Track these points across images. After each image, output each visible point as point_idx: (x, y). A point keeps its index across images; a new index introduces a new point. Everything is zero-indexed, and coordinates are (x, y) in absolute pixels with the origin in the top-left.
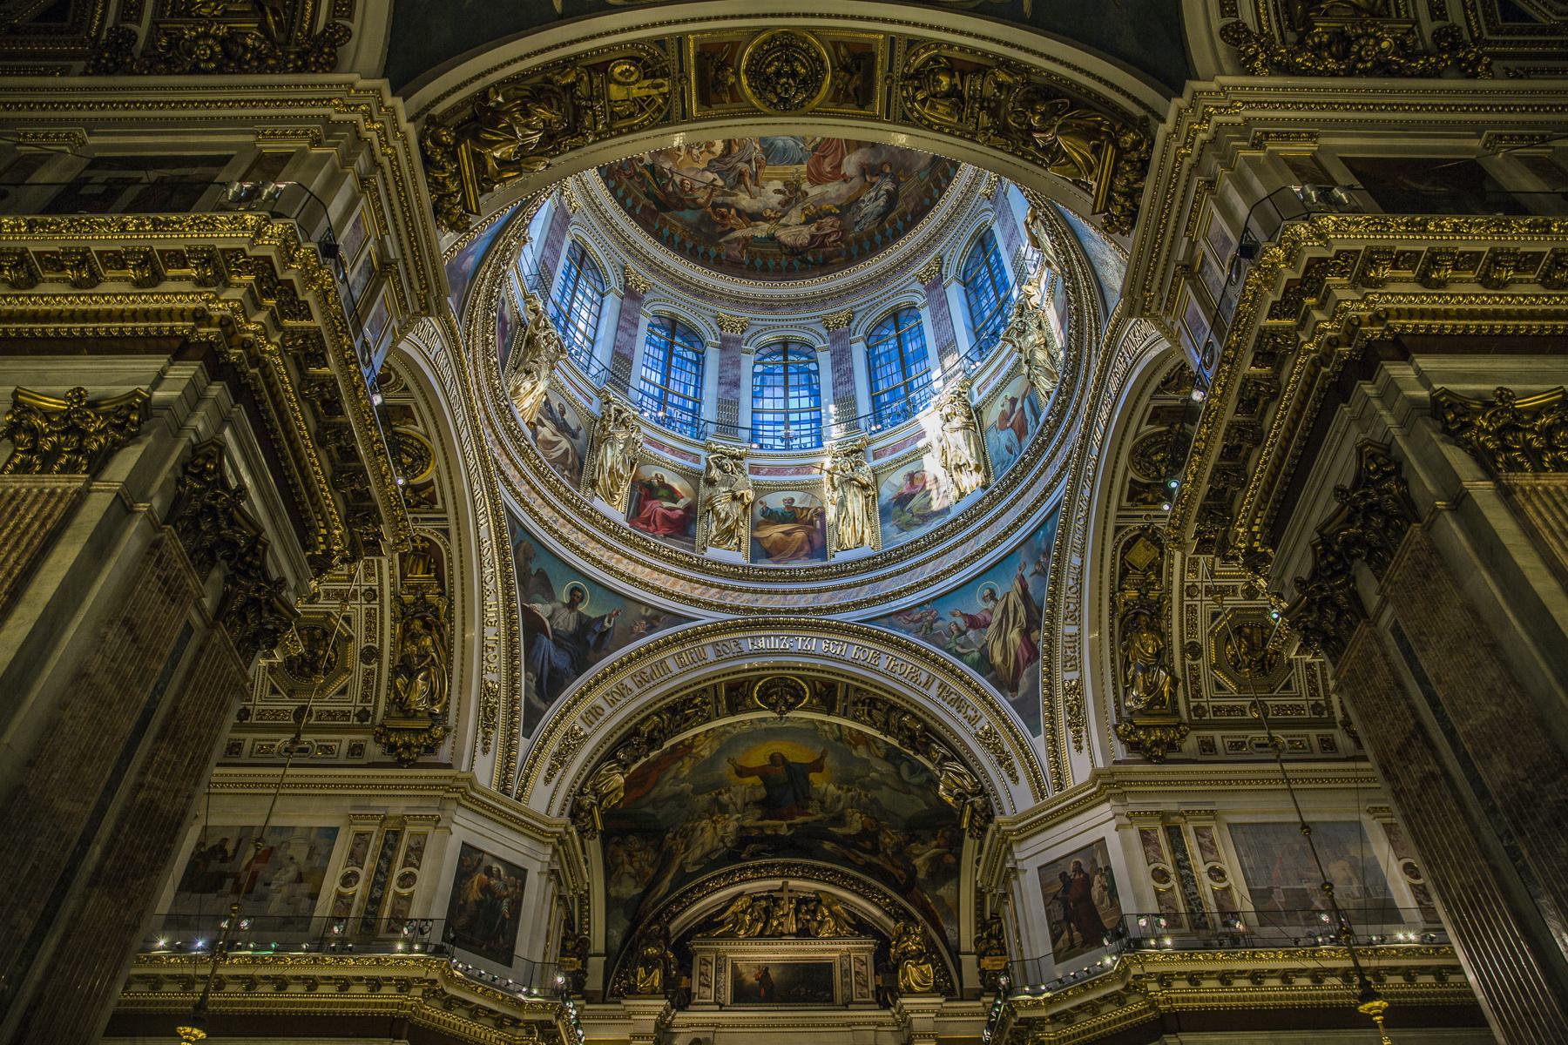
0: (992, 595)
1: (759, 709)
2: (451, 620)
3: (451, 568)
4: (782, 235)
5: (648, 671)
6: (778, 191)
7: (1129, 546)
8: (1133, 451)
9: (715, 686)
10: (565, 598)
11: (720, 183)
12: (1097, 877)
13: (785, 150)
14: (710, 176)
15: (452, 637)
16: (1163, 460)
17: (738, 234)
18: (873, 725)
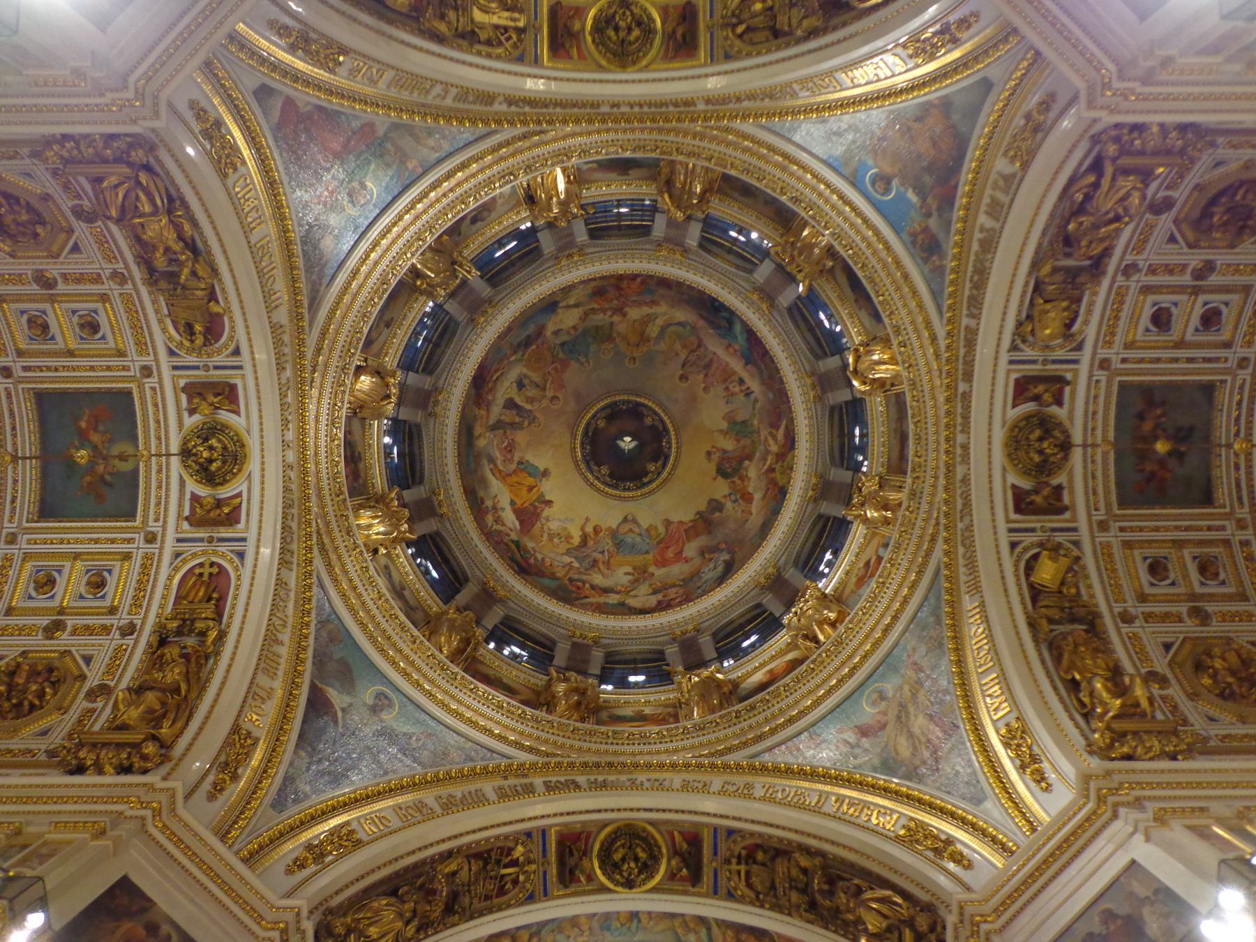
0: (882, 697)
1: (603, 889)
2: (217, 654)
3: (235, 597)
4: (632, 602)
5: (459, 795)
6: (628, 574)
8: (1006, 445)
9: (544, 832)
10: (370, 701)
11: (576, 565)
12: (1146, 912)
13: (633, 546)
14: (567, 559)
15: (212, 672)
16: (1041, 439)
17: (591, 600)
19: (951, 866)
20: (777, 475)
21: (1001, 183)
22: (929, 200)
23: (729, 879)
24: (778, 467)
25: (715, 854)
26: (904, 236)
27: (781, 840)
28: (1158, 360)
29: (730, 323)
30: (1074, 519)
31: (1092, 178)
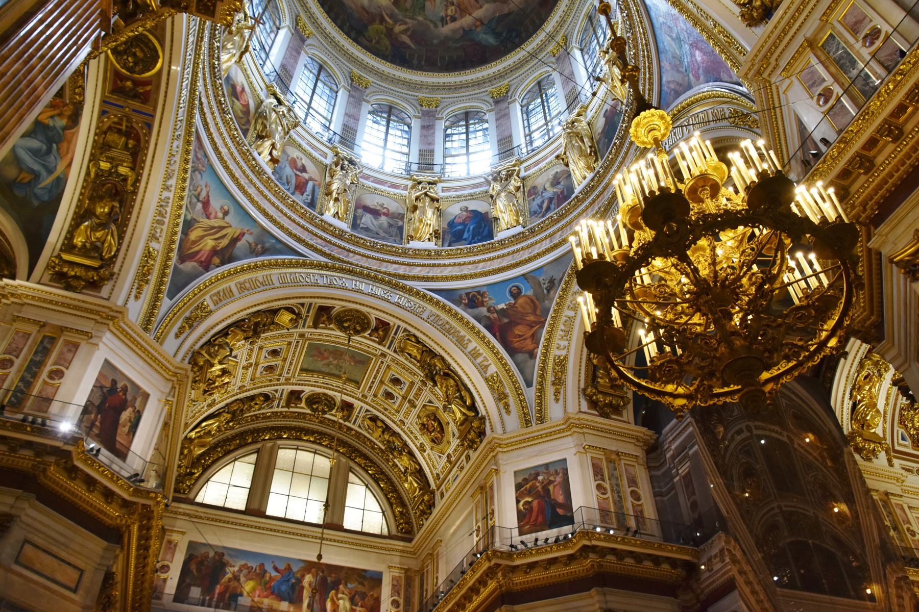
0: (226, 213)
7: (289, 310)
8: (357, 311)
12: (130, 410)
18: (101, 132)
19: (136, 285)
20: (377, 26)
21: (486, 363)
22: (495, 315)
23: (115, 116)
24: (382, 27)
25: (134, 110)
26: (484, 289)
27: (144, 162)
28: (378, 372)
29: (497, 35)
30: (309, 327)
31: (468, 402)
